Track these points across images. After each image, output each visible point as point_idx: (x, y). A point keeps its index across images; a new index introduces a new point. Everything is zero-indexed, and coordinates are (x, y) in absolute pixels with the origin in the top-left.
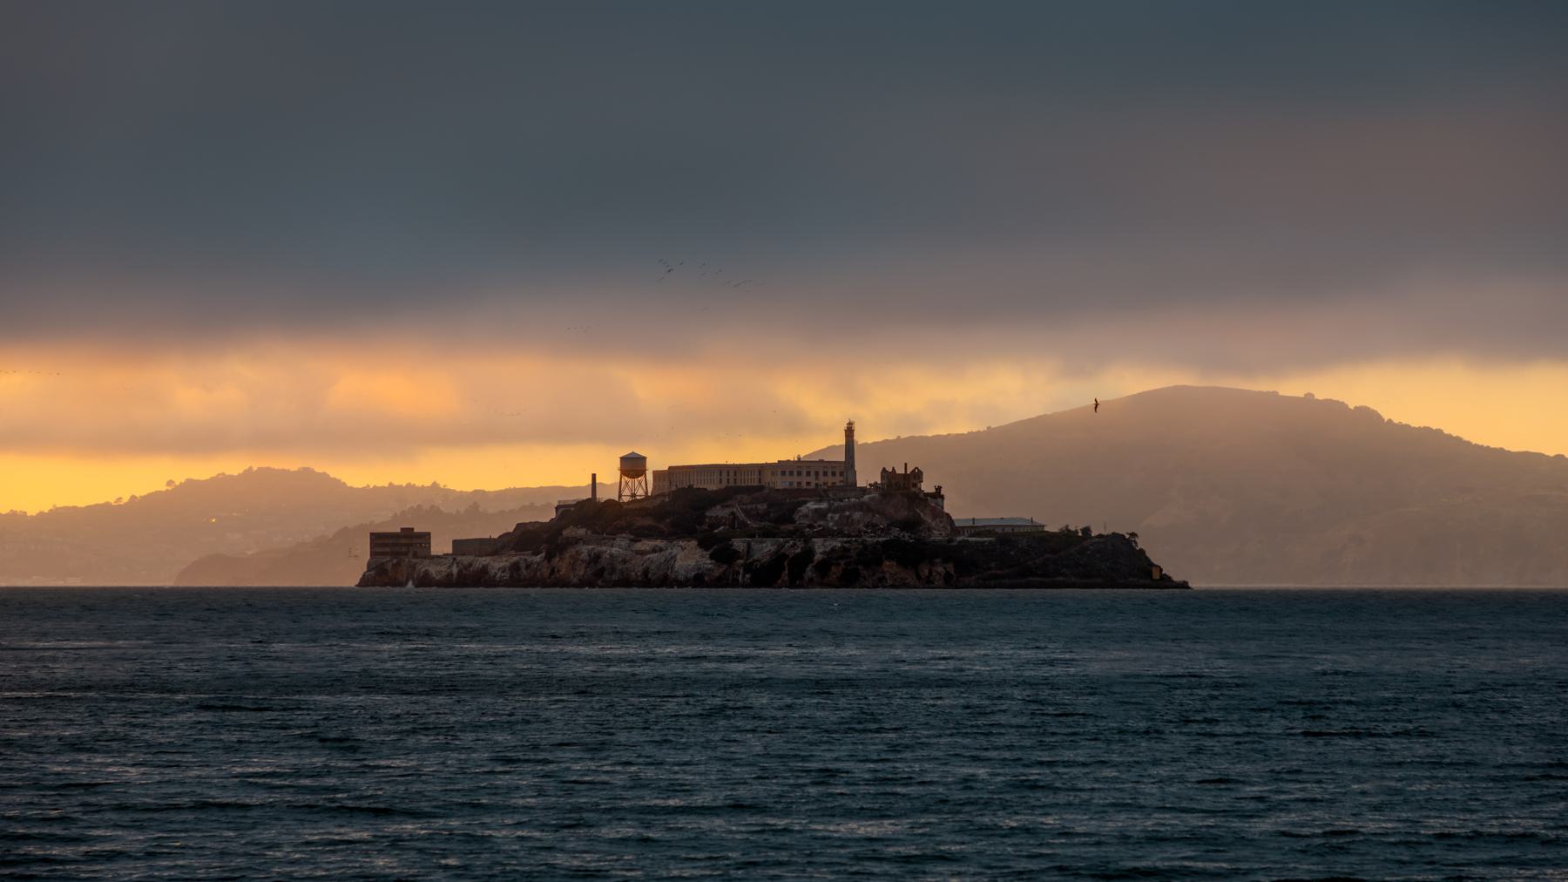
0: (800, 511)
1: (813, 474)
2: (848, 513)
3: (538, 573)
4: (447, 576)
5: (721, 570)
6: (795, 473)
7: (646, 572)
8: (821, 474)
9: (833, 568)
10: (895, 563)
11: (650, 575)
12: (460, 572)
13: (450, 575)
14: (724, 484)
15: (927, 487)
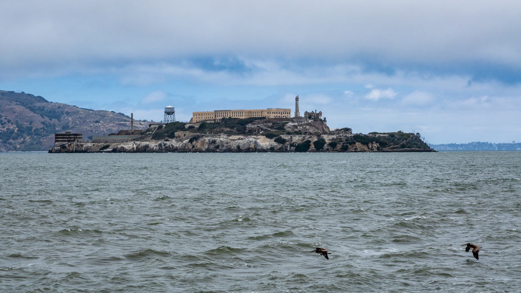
0: (287, 126)
1: (280, 113)
2: (305, 127)
3: (186, 147)
4: (133, 148)
5: (280, 146)
6: (276, 113)
7: (238, 147)
8: (282, 113)
9: (338, 145)
10: (360, 143)
11: (241, 148)
12: (137, 148)
13: (133, 148)
14: (248, 117)
15: (322, 118)
